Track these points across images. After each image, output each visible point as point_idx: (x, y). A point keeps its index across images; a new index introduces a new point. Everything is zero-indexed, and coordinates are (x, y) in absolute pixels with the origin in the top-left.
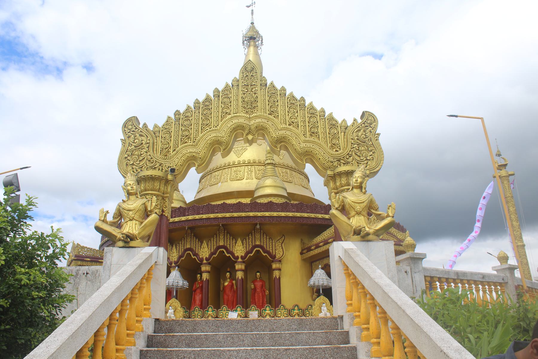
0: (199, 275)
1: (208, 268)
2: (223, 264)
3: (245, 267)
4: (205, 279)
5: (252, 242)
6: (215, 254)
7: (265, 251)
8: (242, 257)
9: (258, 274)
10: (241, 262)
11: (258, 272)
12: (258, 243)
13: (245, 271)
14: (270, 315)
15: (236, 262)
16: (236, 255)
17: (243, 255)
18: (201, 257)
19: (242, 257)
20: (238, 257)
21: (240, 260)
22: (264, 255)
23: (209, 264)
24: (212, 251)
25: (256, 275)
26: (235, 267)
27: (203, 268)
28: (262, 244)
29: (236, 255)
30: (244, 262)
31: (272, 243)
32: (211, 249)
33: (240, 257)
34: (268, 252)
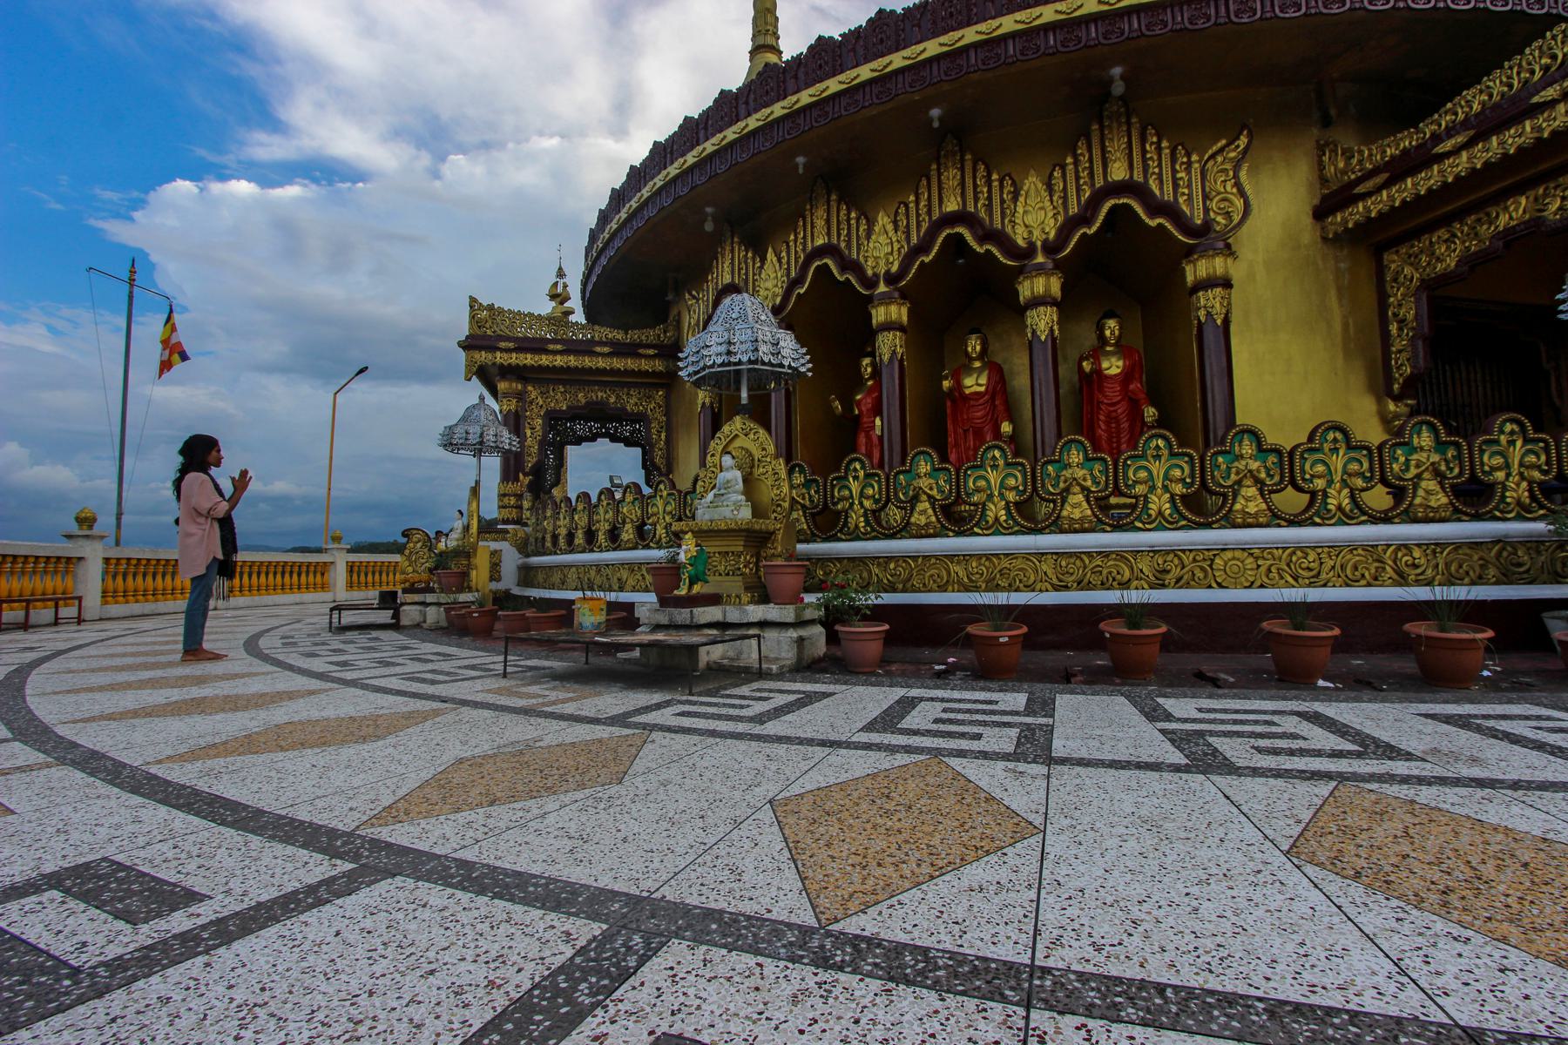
0: (866, 361)
1: (898, 312)
2: (965, 288)
4: (886, 358)
5: (1091, 175)
6: (927, 251)
7: (1157, 208)
9: (1112, 323)
12: (1118, 172)
14: (1259, 483)
15: (1020, 271)
18: (870, 272)
22: (1153, 223)
23: (904, 295)
24: (914, 240)
27: (879, 315)
28: (1138, 177)
31: (1189, 164)
32: (908, 233)
33: (1039, 244)
34: (1171, 211)
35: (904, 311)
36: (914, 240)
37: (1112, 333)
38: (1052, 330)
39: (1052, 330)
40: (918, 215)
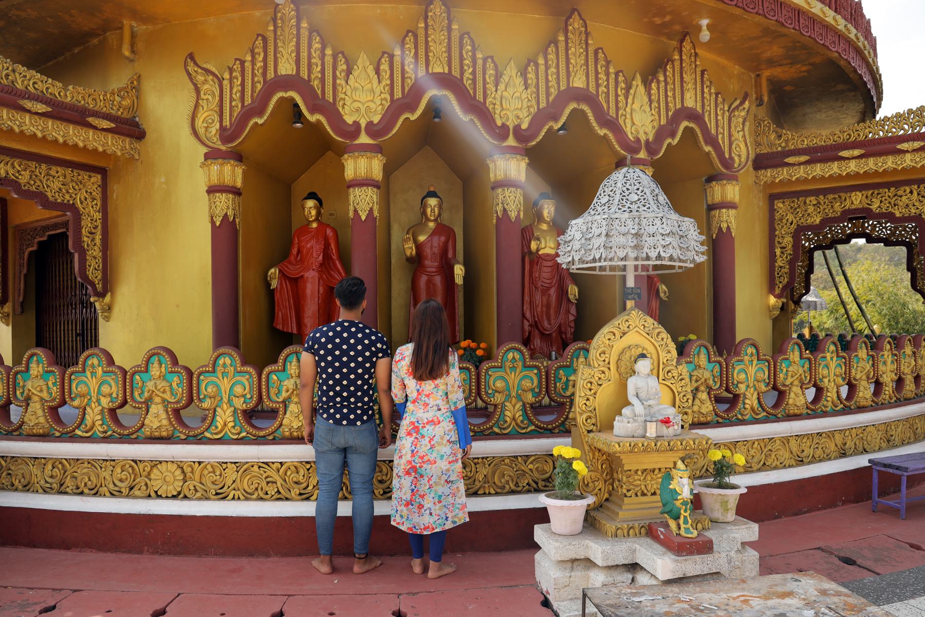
3: (388, 170)
6: (260, 113)
8: (370, 124)
9: (432, 202)
10: (365, 148)
11: (432, 194)
13: (384, 187)
16: (349, 120)
17: (376, 119)
19: (371, 129)
20: (355, 130)
21: (364, 139)
25: (423, 205)
26: (342, 168)
29: (349, 120)
30: (376, 149)
33: (363, 125)
35: (239, 171)
36: (248, 101)
37: (433, 211)
38: (371, 210)
39: (371, 210)
40: (253, 75)
